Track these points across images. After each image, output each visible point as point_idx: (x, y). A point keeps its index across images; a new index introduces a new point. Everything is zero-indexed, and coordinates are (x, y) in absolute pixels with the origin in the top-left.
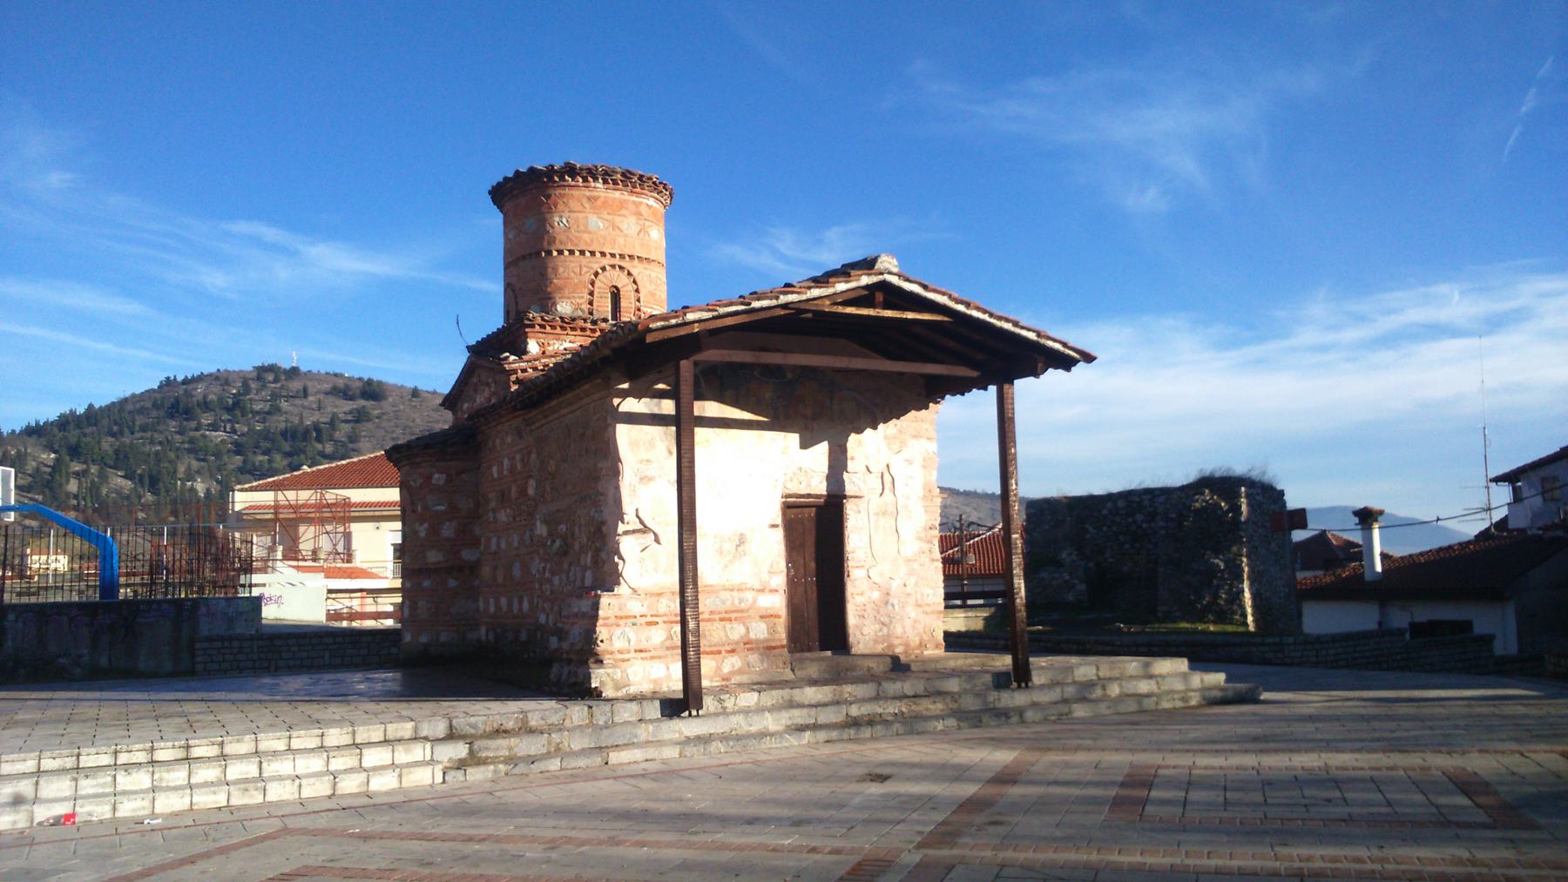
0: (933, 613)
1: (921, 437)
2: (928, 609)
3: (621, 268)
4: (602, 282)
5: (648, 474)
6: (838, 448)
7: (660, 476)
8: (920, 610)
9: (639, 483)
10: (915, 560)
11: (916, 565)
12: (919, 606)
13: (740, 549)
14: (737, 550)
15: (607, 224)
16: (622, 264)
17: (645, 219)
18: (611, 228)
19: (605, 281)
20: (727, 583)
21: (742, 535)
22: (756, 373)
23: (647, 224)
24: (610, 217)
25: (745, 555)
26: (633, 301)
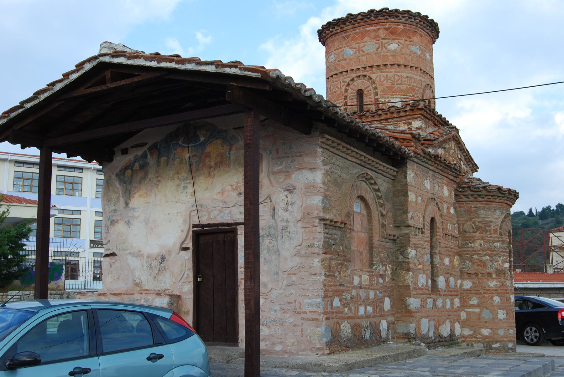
0: (308, 319)
1: (303, 168)
2: (305, 316)
3: (365, 76)
4: (352, 89)
5: (115, 218)
6: (231, 187)
7: (120, 220)
8: (299, 316)
9: (110, 225)
10: (295, 274)
11: (294, 278)
12: (299, 313)
13: (162, 265)
14: (160, 265)
15: (354, 50)
16: (365, 74)
17: (383, 39)
18: (358, 52)
19: (354, 88)
20: (156, 289)
21: (162, 255)
22: (180, 142)
23: (384, 41)
24: (357, 45)
25: (165, 269)
26: (372, 95)
